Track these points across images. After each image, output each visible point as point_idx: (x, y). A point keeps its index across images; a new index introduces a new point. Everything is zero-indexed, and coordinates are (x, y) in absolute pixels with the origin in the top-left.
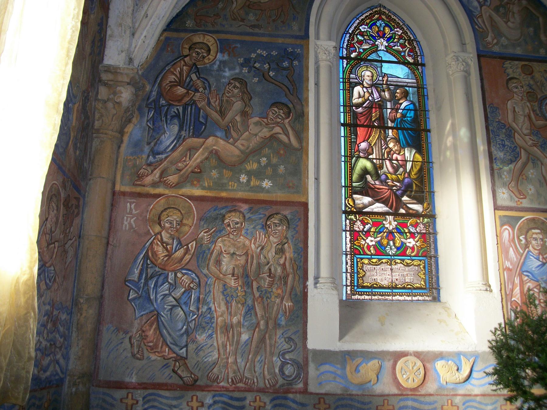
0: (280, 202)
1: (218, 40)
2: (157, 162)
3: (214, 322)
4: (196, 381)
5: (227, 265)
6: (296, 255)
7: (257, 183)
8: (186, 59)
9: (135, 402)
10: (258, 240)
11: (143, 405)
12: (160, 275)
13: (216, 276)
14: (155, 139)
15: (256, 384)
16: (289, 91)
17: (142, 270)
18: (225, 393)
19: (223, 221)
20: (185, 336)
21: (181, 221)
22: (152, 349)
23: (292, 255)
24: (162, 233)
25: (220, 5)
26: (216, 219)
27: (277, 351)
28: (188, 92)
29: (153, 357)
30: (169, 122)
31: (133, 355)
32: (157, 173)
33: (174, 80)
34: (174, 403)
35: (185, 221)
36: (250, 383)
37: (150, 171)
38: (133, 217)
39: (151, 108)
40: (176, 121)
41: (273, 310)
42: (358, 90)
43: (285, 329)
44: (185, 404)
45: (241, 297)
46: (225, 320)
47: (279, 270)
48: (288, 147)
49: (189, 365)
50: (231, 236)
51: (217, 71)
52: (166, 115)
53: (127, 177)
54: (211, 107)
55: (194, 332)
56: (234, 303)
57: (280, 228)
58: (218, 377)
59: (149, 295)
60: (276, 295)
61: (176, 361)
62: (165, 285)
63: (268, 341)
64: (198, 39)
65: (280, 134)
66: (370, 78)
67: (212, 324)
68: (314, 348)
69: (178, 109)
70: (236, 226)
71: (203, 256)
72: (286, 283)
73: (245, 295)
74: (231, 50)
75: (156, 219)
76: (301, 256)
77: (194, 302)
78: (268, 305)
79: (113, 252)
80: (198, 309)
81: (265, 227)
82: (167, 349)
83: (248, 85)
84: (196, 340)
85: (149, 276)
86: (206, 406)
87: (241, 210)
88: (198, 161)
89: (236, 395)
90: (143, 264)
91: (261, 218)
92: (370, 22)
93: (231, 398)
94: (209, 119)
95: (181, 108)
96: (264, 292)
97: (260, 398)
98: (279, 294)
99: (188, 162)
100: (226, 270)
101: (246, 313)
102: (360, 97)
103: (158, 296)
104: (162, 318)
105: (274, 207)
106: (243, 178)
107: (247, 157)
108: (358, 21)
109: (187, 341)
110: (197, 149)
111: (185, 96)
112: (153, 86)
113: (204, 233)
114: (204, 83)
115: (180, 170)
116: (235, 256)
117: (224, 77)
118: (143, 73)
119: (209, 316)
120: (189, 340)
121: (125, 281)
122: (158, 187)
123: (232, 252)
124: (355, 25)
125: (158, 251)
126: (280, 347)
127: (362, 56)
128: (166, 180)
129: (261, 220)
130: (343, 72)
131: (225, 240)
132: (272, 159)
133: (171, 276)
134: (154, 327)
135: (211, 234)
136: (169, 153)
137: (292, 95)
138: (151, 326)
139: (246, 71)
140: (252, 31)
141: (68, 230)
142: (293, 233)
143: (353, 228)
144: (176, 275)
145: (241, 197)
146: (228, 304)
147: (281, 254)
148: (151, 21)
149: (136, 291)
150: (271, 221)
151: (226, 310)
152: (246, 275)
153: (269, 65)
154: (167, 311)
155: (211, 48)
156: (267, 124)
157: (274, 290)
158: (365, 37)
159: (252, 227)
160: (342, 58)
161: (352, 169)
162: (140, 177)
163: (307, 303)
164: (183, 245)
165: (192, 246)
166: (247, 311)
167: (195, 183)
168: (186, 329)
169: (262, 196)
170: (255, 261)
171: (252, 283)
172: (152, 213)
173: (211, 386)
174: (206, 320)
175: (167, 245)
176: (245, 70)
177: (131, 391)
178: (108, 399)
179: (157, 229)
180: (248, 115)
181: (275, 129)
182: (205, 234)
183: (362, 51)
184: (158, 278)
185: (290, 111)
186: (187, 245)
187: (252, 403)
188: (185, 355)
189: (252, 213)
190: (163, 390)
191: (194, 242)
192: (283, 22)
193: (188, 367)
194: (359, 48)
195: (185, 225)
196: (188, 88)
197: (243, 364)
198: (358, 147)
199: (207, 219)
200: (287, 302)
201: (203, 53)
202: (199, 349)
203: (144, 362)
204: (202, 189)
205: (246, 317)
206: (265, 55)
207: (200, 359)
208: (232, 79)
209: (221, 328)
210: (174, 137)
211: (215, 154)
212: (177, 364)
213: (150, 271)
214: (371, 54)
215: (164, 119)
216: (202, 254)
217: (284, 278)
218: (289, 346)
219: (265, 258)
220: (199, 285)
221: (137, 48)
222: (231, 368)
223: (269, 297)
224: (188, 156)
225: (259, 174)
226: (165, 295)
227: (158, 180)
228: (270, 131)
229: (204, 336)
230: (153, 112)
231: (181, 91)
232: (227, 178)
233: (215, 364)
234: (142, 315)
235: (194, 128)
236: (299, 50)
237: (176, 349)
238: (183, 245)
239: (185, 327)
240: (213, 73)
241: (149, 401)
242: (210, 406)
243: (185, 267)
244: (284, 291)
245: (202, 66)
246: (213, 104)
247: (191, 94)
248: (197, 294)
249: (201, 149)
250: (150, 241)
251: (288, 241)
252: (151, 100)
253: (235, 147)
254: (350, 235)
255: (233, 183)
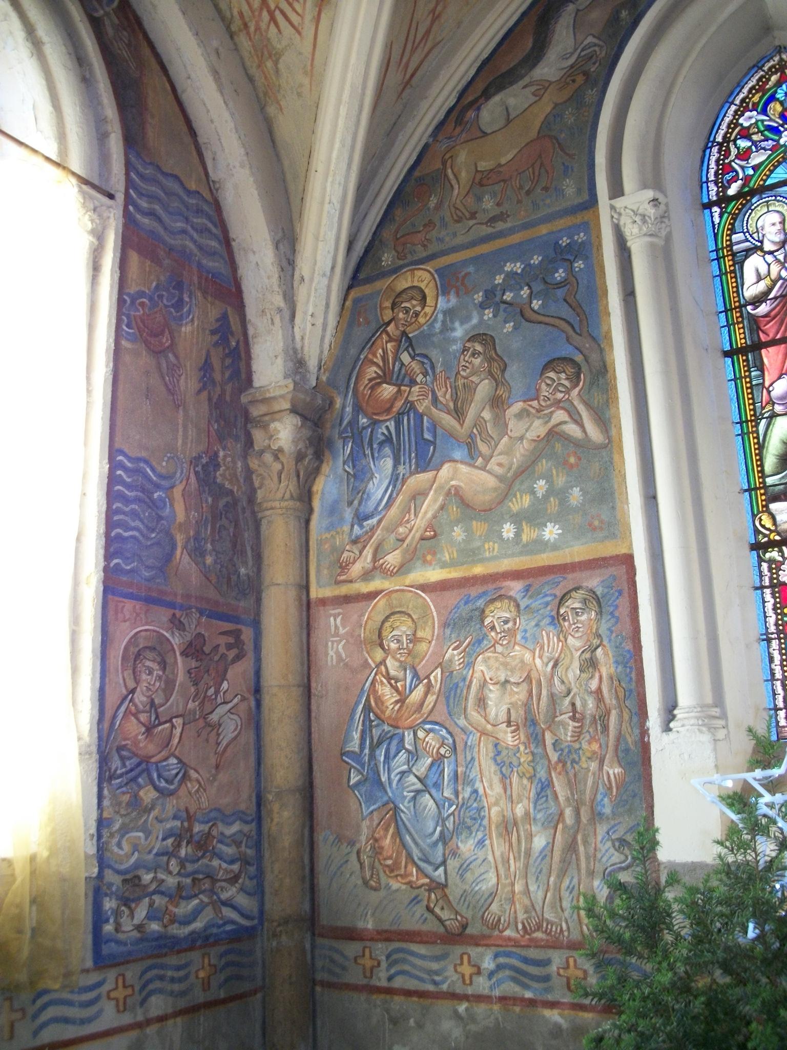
0: (580, 563)
1: (436, 271)
2: (367, 533)
3: (484, 817)
4: (464, 927)
5: (496, 706)
6: (620, 668)
7: (534, 535)
8: (389, 329)
9: (376, 964)
10: (546, 649)
11: (388, 970)
12: (391, 738)
13: (480, 728)
14: (358, 493)
15: (566, 934)
16: (573, 327)
17: (363, 732)
18: (514, 950)
19: (483, 622)
20: (440, 845)
21: (414, 635)
22: (392, 871)
23: (612, 670)
24: (388, 662)
25: (433, 202)
26: (470, 619)
27: (599, 868)
28: (399, 391)
29: (395, 885)
30: (376, 455)
31: (366, 883)
32: (368, 553)
33: (374, 375)
34: (435, 966)
35: (420, 634)
36: (556, 932)
37: (358, 553)
38: (339, 642)
39: (347, 437)
40: (387, 450)
41: (585, 784)
42: (753, 264)
43: (612, 823)
44: (451, 968)
45: (526, 765)
46: (503, 810)
47: (591, 703)
48: (582, 446)
49: (451, 898)
50: (499, 648)
51: (442, 332)
52: (371, 444)
53: (325, 572)
54: (439, 406)
55: (454, 837)
56: (515, 778)
57: (584, 617)
58: (499, 920)
59: (379, 775)
60: (589, 755)
61: (430, 890)
62: (400, 754)
63: (581, 849)
64: (403, 283)
65: (565, 422)
66: (779, 227)
67: (482, 820)
68: (672, 859)
69: (387, 428)
70: (506, 627)
71: (455, 695)
72: (605, 728)
73: (533, 761)
74: (459, 284)
75: (375, 637)
76: (631, 668)
77: (449, 781)
78: (575, 775)
79: (318, 707)
80: (457, 794)
81: (557, 619)
82: (414, 870)
83: (497, 341)
84: (459, 852)
85: (375, 741)
86: (486, 973)
87: (512, 593)
88: (429, 515)
89: (533, 953)
90: (363, 721)
91: (547, 604)
92: (761, 98)
93: (526, 960)
94: (439, 431)
95: (393, 423)
96: (566, 750)
97: (575, 961)
98: (594, 753)
99: (413, 523)
100: (497, 715)
101: (538, 794)
102: (759, 278)
103: (392, 776)
104: (402, 815)
105: (570, 576)
106: (508, 530)
107: (510, 487)
108: (733, 108)
109: (444, 855)
110: (424, 494)
111: (395, 399)
112: (346, 396)
113: (453, 650)
114: (423, 363)
115: (403, 540)
116: (508, 686)
117: (454, 341)
118: (328, 379)
119: (475, 805)
120: (447, 852)
121: (342, 754)
122: (373, 578)
123: (502, 679)
124: (727, 120)
125: (383, 695)
126: (604, 859)
127: (751, 184)
128: (382, 564)
129: (549, 608)
130: (716, 235)
131: (489, 658)
132: (555, 478)
133: (409, 737)
134: (391, 831)
135: (464, 650)
136: (384, 513)
137: (580, 335)
138: (386, 830)
139: (491, 315)
140: (493, 230)
141: (211, 691)
142: (610, 625)
143: (777, 578)
144: (415, 734)
145: (509, 568)
146: (505, 779)
147: (591, 670)
148: (314, 285)
149: (358, 771)
150: (568, 607)
151: (502, 791)
152: (531, 721)
153: (530, 288)
154: (409, 802)
155: (427, 291)
156: (538, 411)
157: (585, 745)
158: (755, 137)
159: (533, 623)
160: (708, 206)
161: (761, 447)
162: (344, 567)
163: (650, 767)
164: (422, 677)
165: (435, 677)
166: (539, 790)
167: (429, 557)
168: (442, 833)
169: (545, 559)
170: (544, 692)
171: (543, 735)
172: (368, 627)
173: (490, 937)
174: (471, 814)
175: (396, 682)
176: (488, 314)
177: (368, 944)
178: (336, 957)
179: (379, 654)
180: (503, 404)
181: (554, 416)
182: (455, 652)
183: (751, 172)
184: (389, 744)
185: (580, 369)
186: (428, 677)
187: (561, 971)
188: (443, 880)
189: (531, 597)
190: (417, 943)
191: (439, 670)
192: (546, 189)
193: (450, 902)
194: (743, 168)
195: (421, 640)
196: (399, 382)
197: (540, 894)
198: (769, 392)
199: (455, 624)
200: (611, 767)
201: (414, 306)
202: (464, 869)
203: (382, 893)
204: (442, 568)
205: (539, 802)
206: (519, 271)
207: (467, 887)
208: (469, 341)
209: (497, 827)
210: (387, 481)
211: (456, 495)
212: (433, 896)
213: (376, 733)
214: (772, 172)
215: (368, 452)
216: (453, 691)
217: (602, 719)
218: (623, 858)
219: (563, 682)
220: (454, 749)
221: (306, 338)
222: (520, 903)
223: (577, 759)
224: (413, 511)
225: (535, 516)
226: (403, 773)
227: (370, 566)
228: (547, 422)
229: (471, 843)
230: (350, 445)
231: (388, 390)
232: (480, 536)
233: (493, 895)
234: (372, 812)
235: (416, 455)
236: (582, 234)
237: (429, 869)
238: (422, 678)
239: (439, 829)
240: (435, 339)
241: (396, 962)
242: (491, 974)
243: (429, 719)
244: (604, 746)
245: (416, 333)
246: (441, 399)
247: (405, 391)
248: (452, 766)
249: (432, 492)
250: (371, 678)
251: (602, 641)
252: (345, 422)
253: (489, 472)
254: (773, 594)
255: (491, 543)
